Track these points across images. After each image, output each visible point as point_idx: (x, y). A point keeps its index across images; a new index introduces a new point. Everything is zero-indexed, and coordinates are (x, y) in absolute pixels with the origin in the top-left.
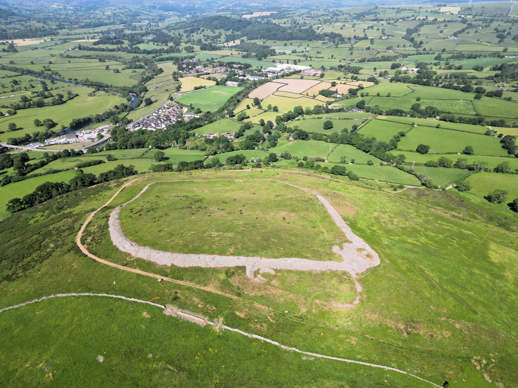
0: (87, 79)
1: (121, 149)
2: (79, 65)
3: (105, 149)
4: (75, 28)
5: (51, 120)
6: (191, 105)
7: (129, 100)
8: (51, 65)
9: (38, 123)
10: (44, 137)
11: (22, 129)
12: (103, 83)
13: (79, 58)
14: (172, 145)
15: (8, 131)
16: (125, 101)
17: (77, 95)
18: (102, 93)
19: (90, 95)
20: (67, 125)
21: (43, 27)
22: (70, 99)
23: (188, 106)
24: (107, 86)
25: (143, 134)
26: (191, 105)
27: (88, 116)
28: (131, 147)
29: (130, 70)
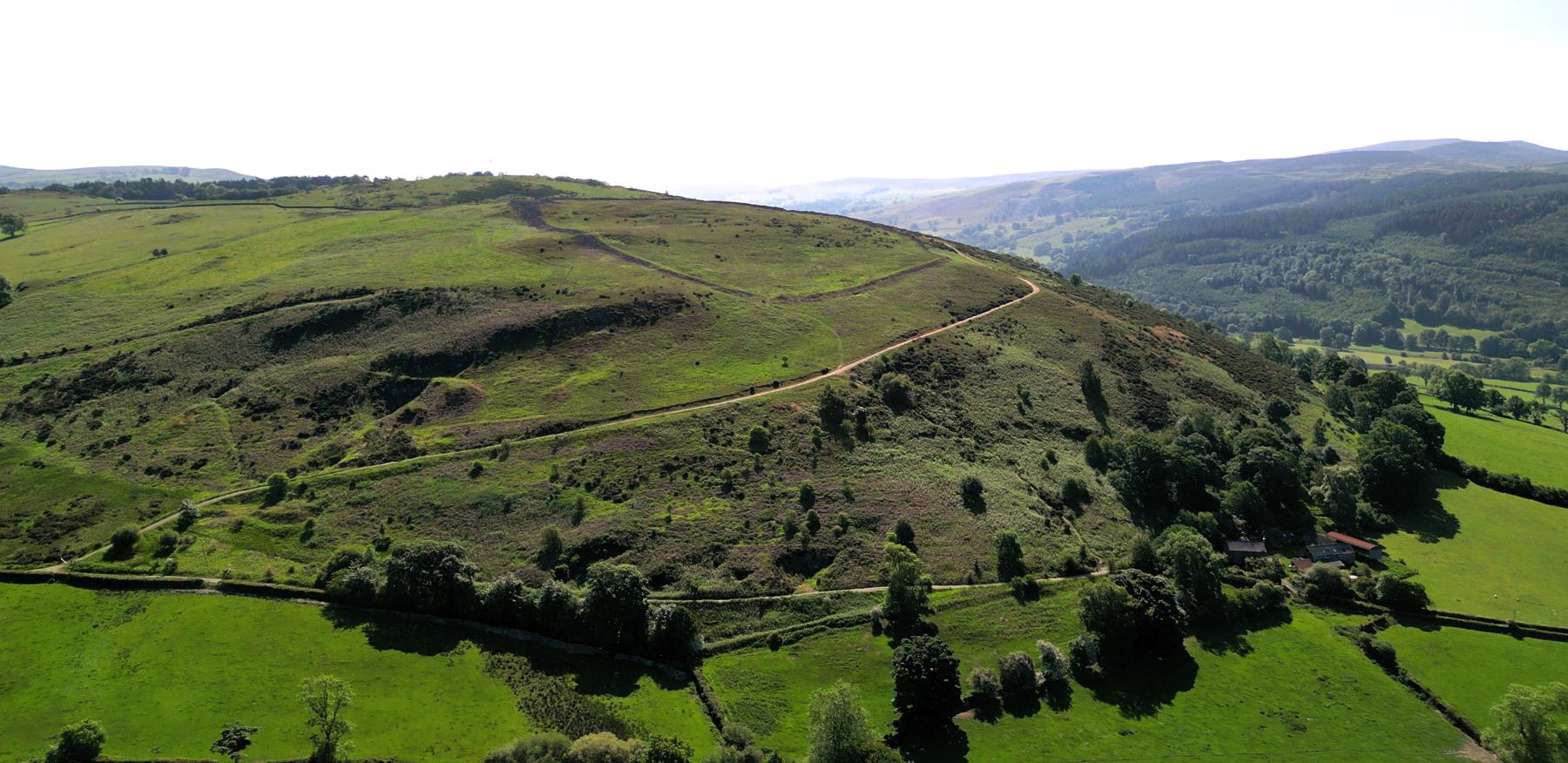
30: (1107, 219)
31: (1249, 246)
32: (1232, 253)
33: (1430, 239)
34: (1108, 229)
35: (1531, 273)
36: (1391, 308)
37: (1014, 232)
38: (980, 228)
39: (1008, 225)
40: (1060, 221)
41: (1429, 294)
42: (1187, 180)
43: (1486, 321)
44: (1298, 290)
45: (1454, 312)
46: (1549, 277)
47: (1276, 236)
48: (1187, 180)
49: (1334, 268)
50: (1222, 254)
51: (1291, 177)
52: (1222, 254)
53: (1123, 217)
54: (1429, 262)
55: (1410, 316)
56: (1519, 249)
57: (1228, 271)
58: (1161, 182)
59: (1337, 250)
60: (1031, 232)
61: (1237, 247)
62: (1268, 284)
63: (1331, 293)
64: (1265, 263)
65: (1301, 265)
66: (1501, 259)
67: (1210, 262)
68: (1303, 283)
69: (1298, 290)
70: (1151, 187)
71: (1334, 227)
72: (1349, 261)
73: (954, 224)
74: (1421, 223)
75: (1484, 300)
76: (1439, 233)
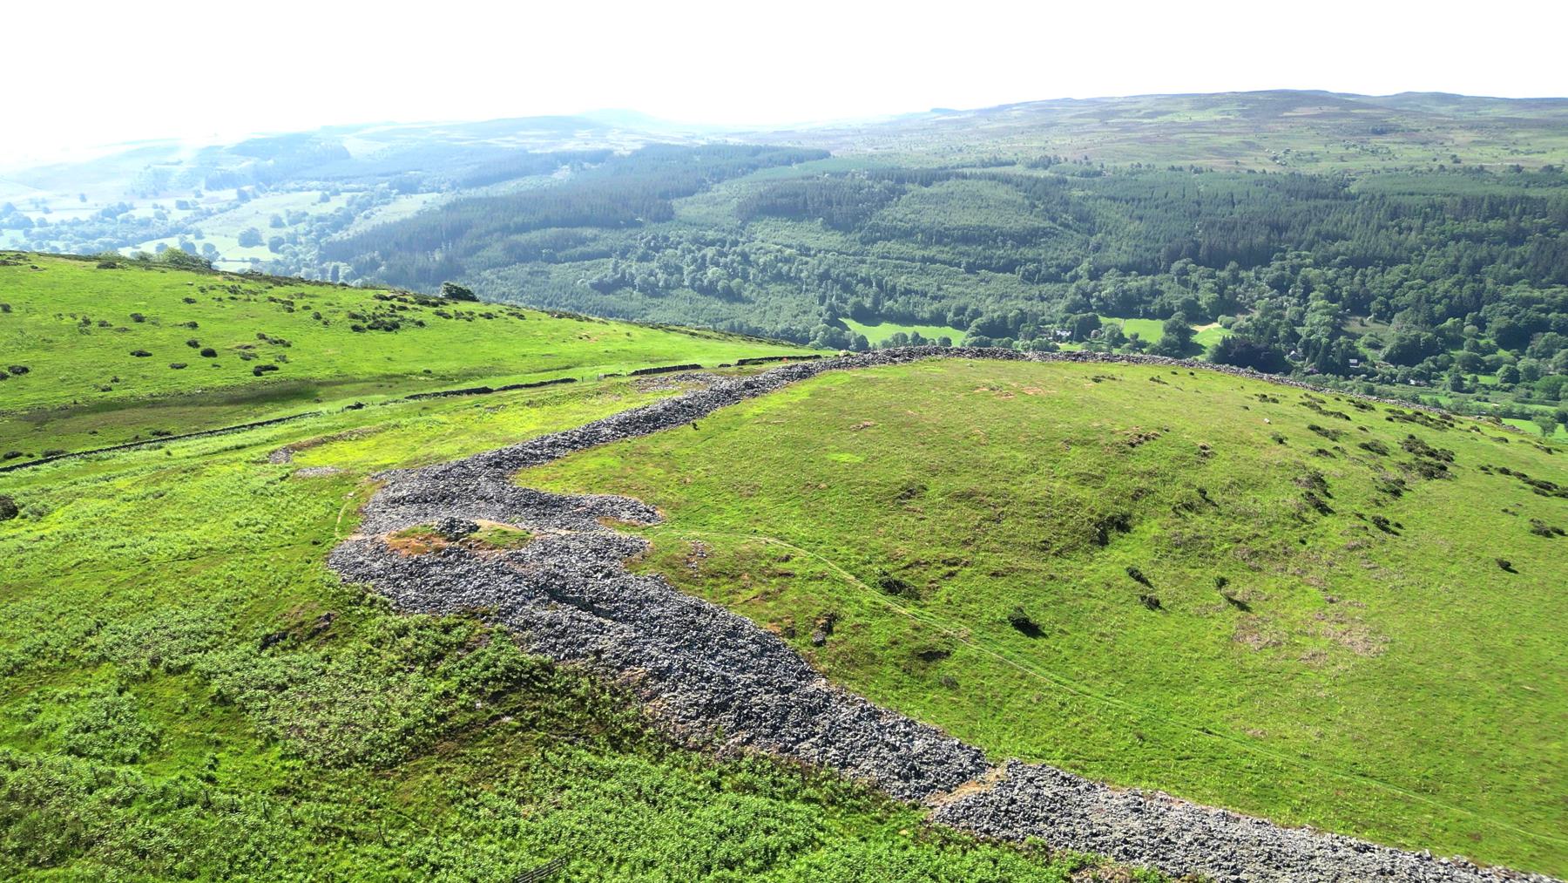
30: (318, 194)
31: (610, 238)
32: (591, 248)
33: (806, 224)
34: (328, 209)
35: (933, 261)
36: (831, 308)
37: (187, 213)
38: (124, 208)
39: (169, 203)
40: (243, 197)
41: (847, 288)
42: (385, 145)
43: (927, 316)
44: (709, 290)
45: (890, 309)
46: (950, 264)
47: (632, 224)
48: (385, 145)
49: (733, 261)
50: (580, 249)
51: (509, 143)
52: (580, 249)
53: (337, 193)
54: (827, 251)
55: (846, 316)
56: (907, 235)
57: (606, 270)
58: (356, 147)
59: (723, 243)
60: (209, 213)
61: (594, 239)
62: (667, 287)
63: (746, 294)
64: (644, 258)
65: (694, 260)
66: (894, 246)
67: (573, 259)
68: (711, 283)
69: (709, 290)
70: (344, 155)
71: (686, 209)
72: (745, 257)
73: (77, 203)
74: (789, 206)
75: (907, 292)
76: (811, 219)
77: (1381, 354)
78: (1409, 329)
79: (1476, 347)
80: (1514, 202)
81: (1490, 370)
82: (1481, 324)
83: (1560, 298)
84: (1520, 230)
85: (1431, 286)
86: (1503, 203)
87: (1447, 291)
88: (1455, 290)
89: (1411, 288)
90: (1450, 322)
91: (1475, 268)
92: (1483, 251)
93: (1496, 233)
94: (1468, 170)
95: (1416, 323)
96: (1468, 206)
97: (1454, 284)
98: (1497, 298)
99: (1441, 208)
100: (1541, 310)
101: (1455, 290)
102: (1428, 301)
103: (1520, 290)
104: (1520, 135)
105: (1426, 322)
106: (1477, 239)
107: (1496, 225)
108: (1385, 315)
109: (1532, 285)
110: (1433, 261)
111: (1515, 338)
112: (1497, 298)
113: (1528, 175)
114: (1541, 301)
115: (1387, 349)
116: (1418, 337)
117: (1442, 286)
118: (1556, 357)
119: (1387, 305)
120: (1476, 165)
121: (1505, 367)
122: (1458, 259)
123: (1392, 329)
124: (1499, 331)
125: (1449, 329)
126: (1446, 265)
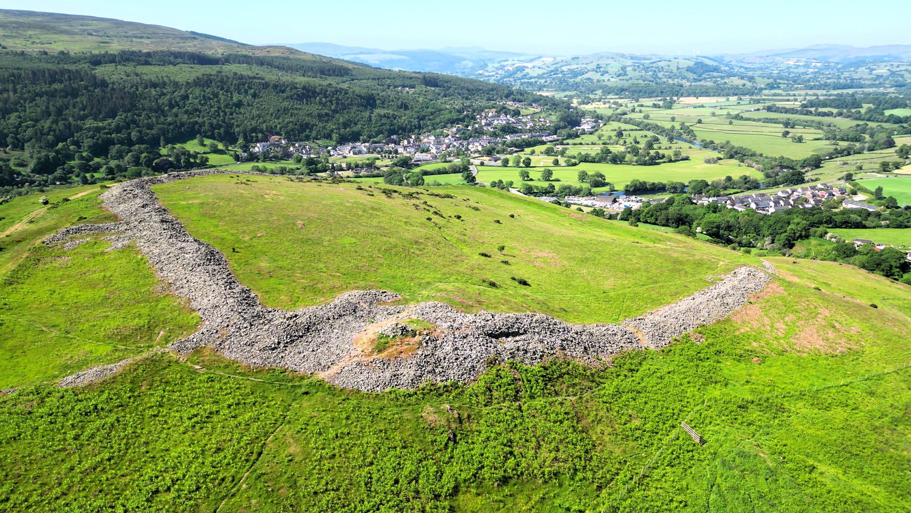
0: (728, 142)
1: (646, 222)
2: (742, 128)
3: (619, 217)
4: (797, 89)
5: (602, 176)
6: (880, 190)
7: (768, 176)
8: (698, 125)
9: (583, 176)
10: (567, 191)
11: (558, 180)
12: (750, 150)
13: (754, 120)
14: (759, 245)
15: (539, 180)
16: (759, 176)
17: (687, 159)
18: (734, 161)
19: (708, 161)
20: (620, 187)
21: (744, 85)
22: (671, 161)
23: (872, 193)
24: (753, 155)
25: (715, 212)
26: (880, 190)
27: (664, 182)
28: (664, 222)
29: (828, 142)
77: (28, 170)
78: (39, 152)
79: (82, 158)
80: (63, 72)
81: (96, 169)
82: (77, 144)
83: (113, 125)
84: (73, 89)
85: (39, 125)
86: (56, 73)
87: (50, 127)
88: (54, 126)
89: (28, 127)
90: (60, 145)
91: (59, 112)
92: (59, 103)
93: (62, 90)
94: (15, 54)
95: (41, 148)
96: (36, 75)
97: (52, 123)
98: (79, 129)
99: (20, 77)
100: (107, 133)
101: (54, 126)
102: (42, 134)
103: (90, 123)
104: (30, 32)
105: (48, 147)
106: (52, 95)
107: (57, 86)
108: (19, 145)
109: (95, 119)
110: (31, 110)
111: (101, 149)
112: (79, 129)
113: (53, 57)
114: (104, 128)
115: (32, 165)
116: (47, 156)
117: (47, 124)
118: (126, 159)
119: (17, 139)
120: (19, 50)
121: (105, 167)
122: (47, 108)
123: (26, 154)
124: (90, 147)
125: (62, 149)
126: (42, 112)
